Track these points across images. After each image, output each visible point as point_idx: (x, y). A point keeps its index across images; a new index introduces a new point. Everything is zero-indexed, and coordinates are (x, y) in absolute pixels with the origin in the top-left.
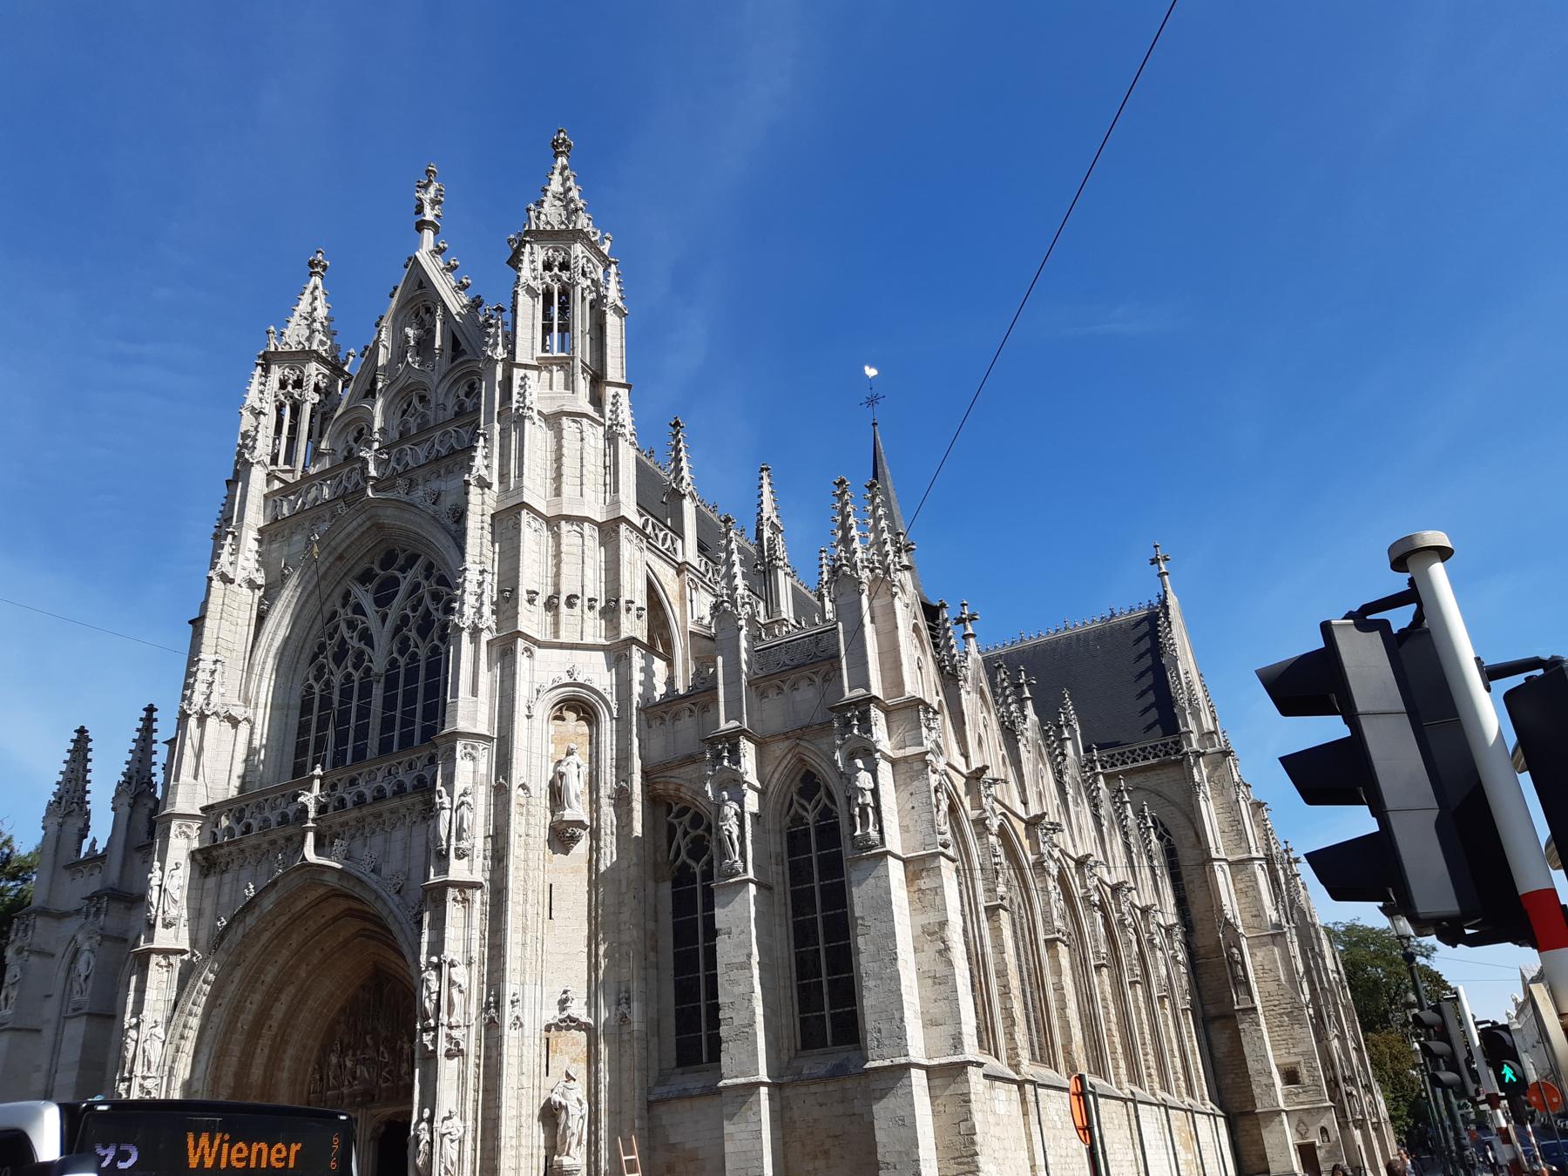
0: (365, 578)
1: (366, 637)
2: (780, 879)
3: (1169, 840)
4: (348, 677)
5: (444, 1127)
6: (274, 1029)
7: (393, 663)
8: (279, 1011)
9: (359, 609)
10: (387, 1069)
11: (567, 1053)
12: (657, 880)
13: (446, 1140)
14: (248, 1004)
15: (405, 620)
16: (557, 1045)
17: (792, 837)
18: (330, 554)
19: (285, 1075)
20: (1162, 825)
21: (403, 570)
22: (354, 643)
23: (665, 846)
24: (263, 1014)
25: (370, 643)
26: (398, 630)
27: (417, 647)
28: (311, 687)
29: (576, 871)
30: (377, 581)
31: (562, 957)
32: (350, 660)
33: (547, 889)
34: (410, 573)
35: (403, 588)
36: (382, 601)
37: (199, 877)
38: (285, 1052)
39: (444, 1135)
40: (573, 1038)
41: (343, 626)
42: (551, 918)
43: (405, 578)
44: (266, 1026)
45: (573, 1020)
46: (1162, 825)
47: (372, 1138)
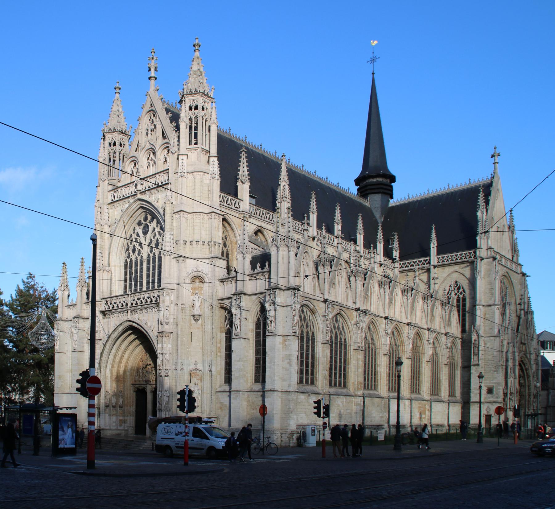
0: (140, 224)
1: (141, 244)
2: (252, 336)
3: (464, 295)
4: (137, 258)
7: (149, 255)
9: (138, 235)
12: (221, 332)
17: (257, 324)
20: (463, 288)
21: (150, 222)
22: (137, 247)
23: (224, 323)
26: (150, 244)
30: (143, 226)
34: (152, 224)
35: (151, 229)
36: (145, 233)
46: (463, 288)
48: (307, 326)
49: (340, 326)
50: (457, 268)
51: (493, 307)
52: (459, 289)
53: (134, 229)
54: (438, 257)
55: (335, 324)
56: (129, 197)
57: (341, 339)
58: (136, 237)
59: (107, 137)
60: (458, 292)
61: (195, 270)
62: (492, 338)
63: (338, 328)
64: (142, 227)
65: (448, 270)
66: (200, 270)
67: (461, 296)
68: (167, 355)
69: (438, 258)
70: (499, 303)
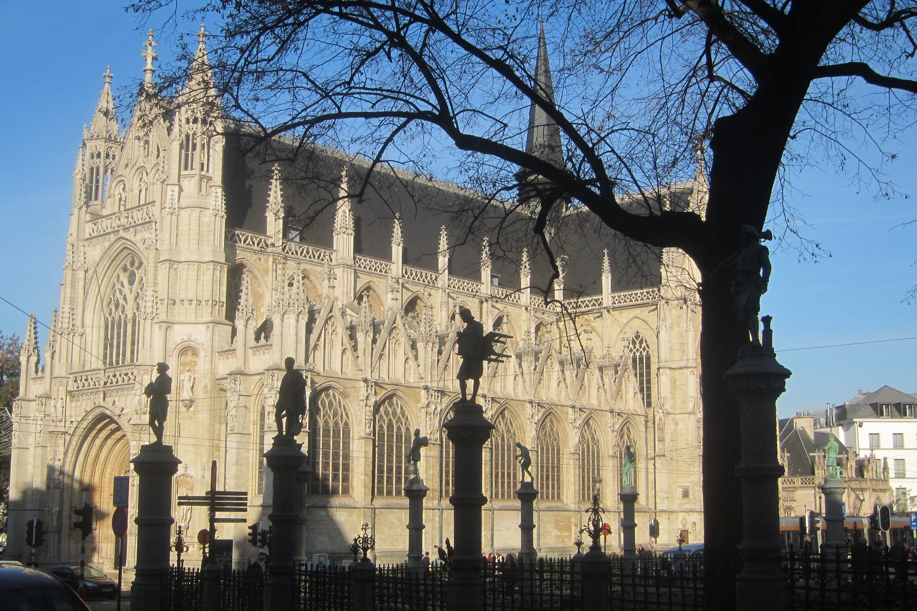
0: (125, 269)
3: (648, 352)
4: (120, 317)
8: (103, 455)
9: (122, 285)
19: (107, 480)
20: (646, 342)
24: (97, 456)
25: (126, 302)
32: (120, 309)
36: (131, 283)
41: (117, 292)
46: (646, 342)
48: (335, 415)
49: (399, 411)
50: (637, 311)
51: (685, 370)
52: (641, 342)
53: (118, 277)
54: (613, 295)
55: (389, 408)
56: (110, 233)
57: (399, 428)
58: (120, 287)
59: (88, 145)
60: (641, 347)
61: (186, 339)
62: (685, 416)
63: (394, 414)
64: (127, 274)
65: (627, 315)
66: (193, 338)
67: (644, 354)
69: (613, 298)
70: (694, 365)
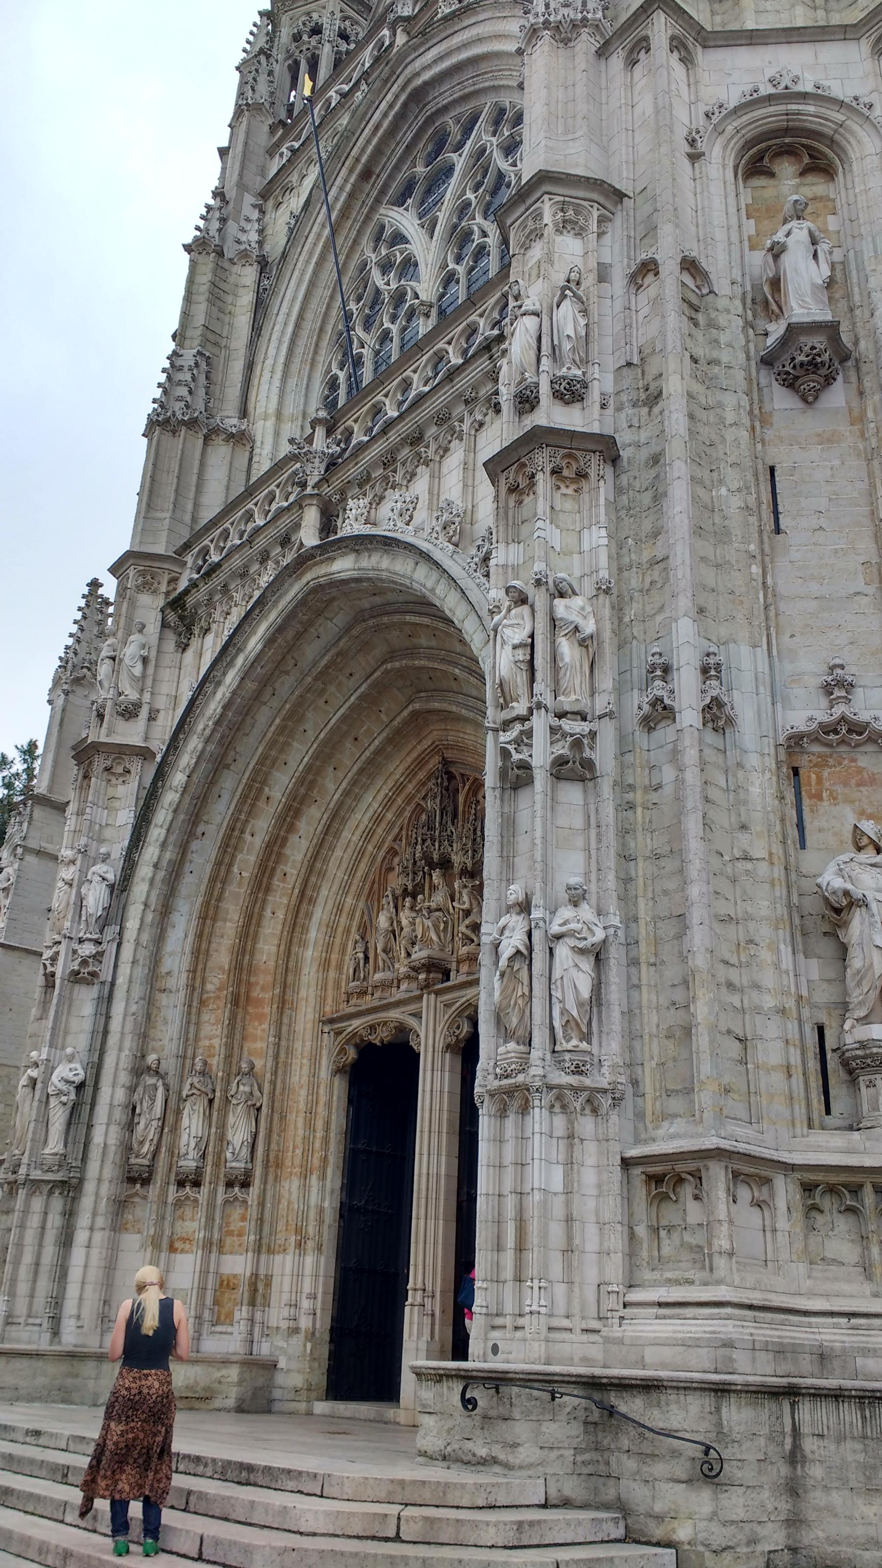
5: (558, 920)
6: (291, 879)
7: (450, 279)
10: (467, 922)
11: (852, 802)
13: (563, 951)
14: (247, 836)
15: (464, 208)
16: (820, 780)
18: (351, 171)
27: (485, 234)
28: (335, 378)
29: (830, 441)
31: (814, 604)
33: (764, 477)
37: (177, 651)
38: (309, 915)
39: (559, 937)
40: (860, 770)
42: (778, 530)
43: (460, 155)
44: (278, 874)
45: (857, 728)
47: (448, 1047)
68: (578, 602)
